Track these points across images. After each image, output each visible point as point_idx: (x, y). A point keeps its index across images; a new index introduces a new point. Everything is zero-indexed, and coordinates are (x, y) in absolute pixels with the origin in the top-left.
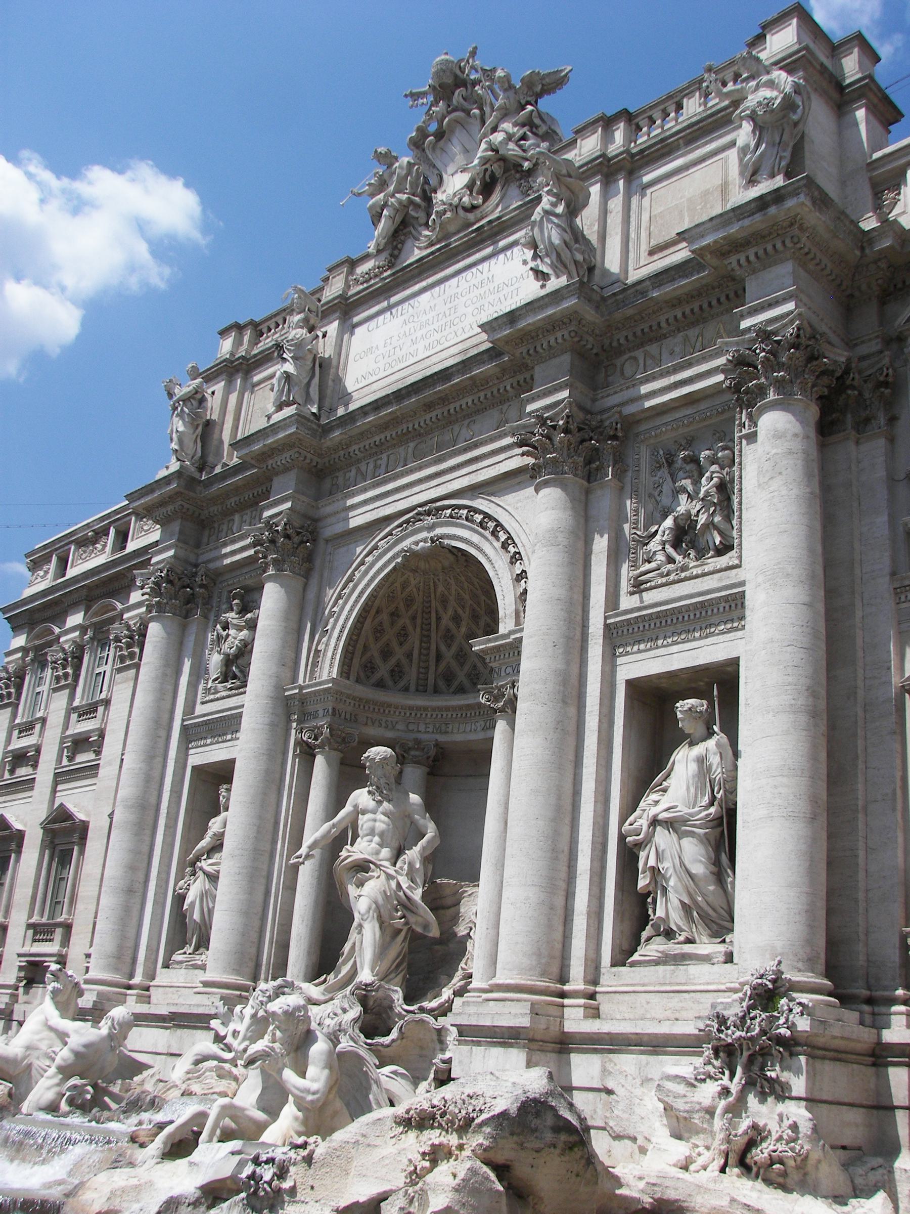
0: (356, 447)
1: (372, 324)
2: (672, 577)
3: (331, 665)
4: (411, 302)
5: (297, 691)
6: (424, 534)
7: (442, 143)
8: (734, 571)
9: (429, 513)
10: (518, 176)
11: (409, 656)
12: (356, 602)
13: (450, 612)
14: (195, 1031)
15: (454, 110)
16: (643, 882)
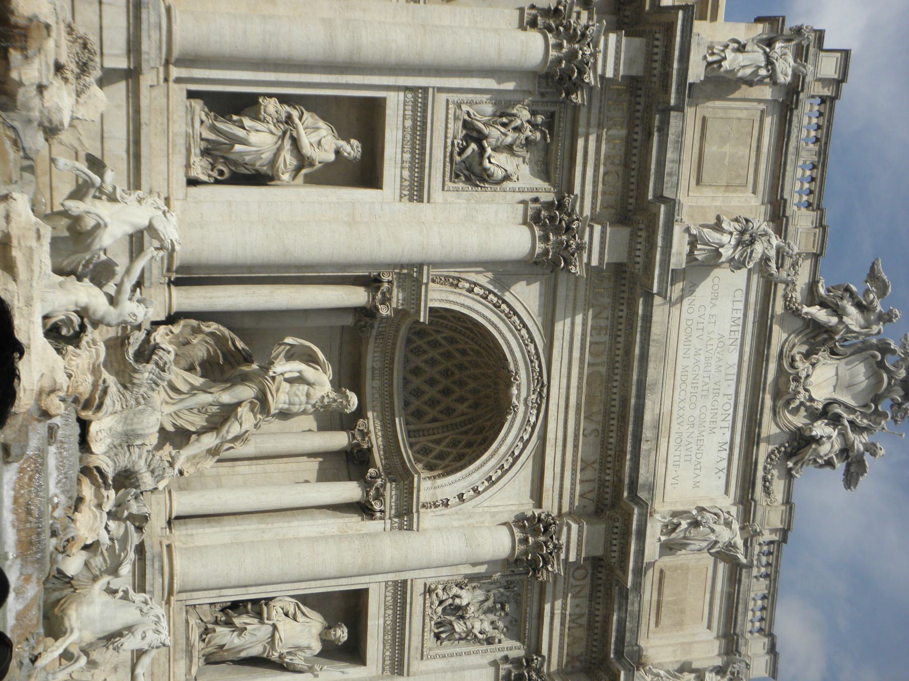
0: (623, 314)
1: (741, 296)
2: (429, 611)
3: (441, 300)
4: (739, 340)
5: (425, 281)
6: (524, 394)
7: (873, 362)
8: (419, 656)
9: (540, 394)
10: (789, 450)
11: (442, 317)
12: (490, 321)
13: (469, 351)
14: (127, 254)
15: (889, 383)
16: (238, 621)
